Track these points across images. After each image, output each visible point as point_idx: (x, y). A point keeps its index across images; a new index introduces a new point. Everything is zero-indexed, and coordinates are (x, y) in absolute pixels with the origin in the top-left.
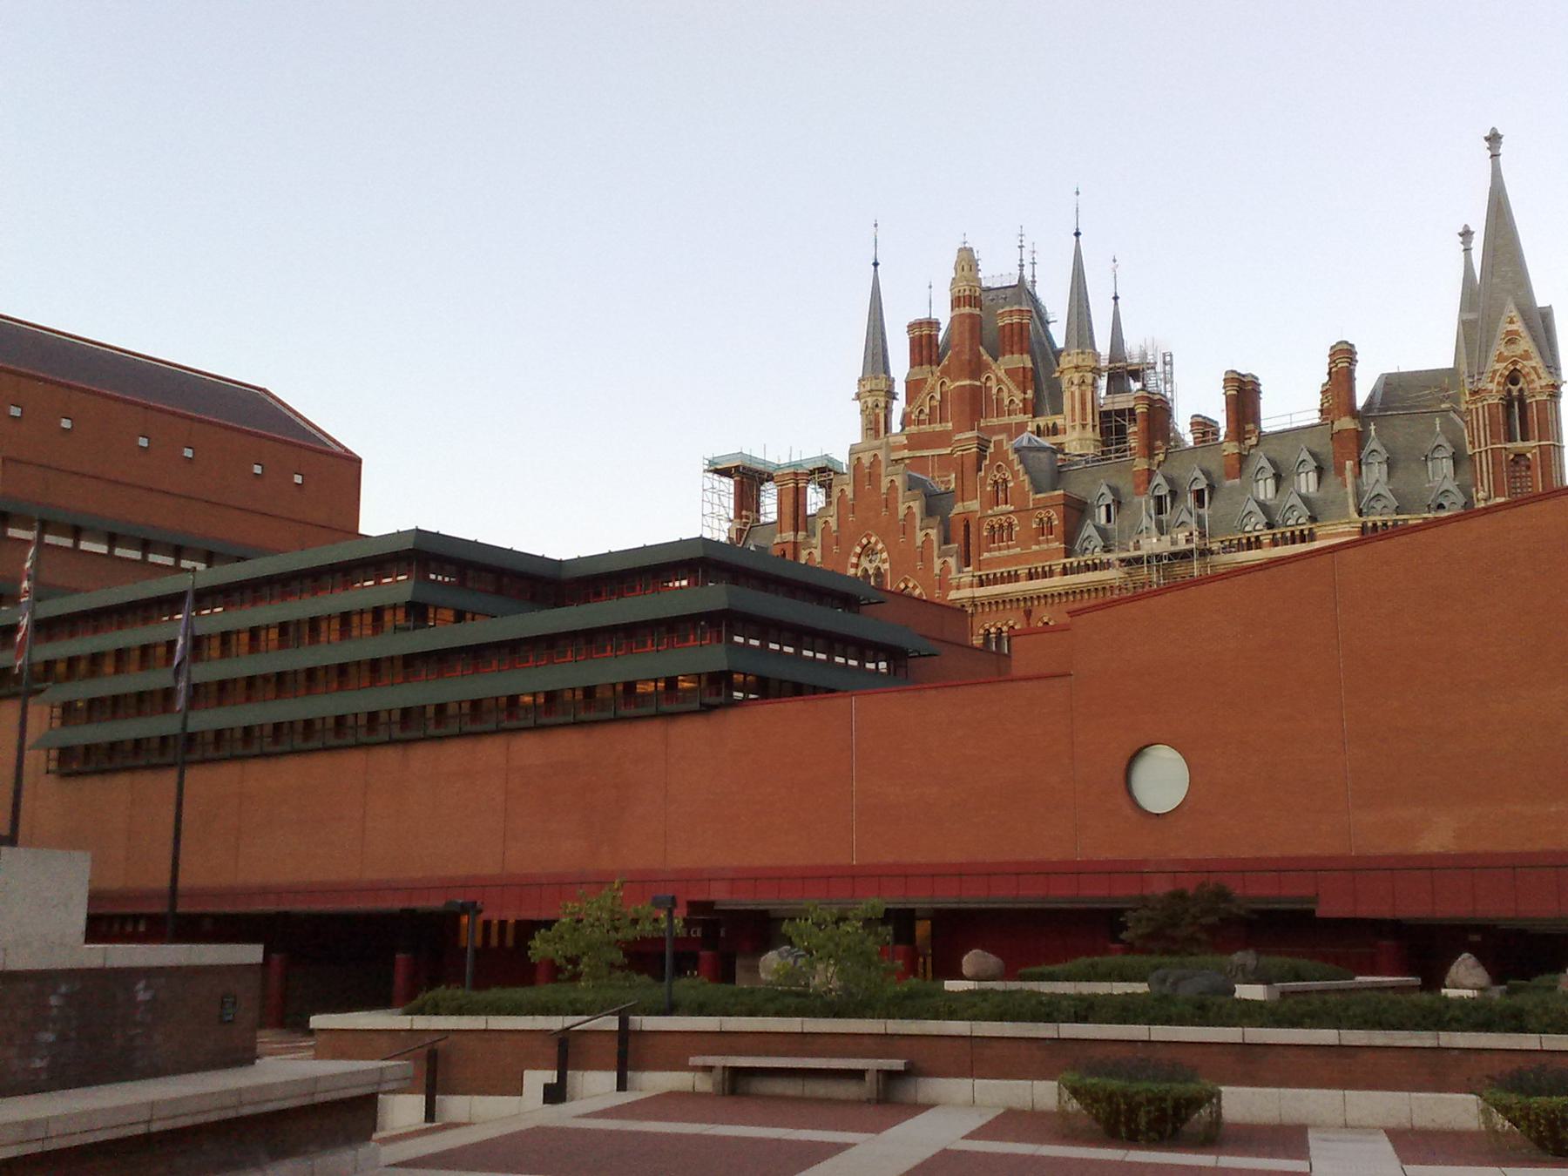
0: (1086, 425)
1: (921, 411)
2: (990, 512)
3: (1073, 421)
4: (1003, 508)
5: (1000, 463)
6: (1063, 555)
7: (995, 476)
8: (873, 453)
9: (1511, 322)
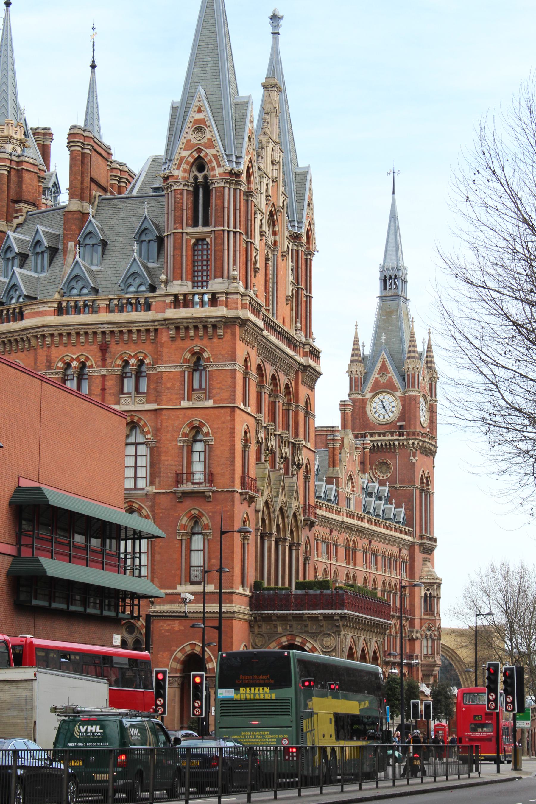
9: (200, 111)
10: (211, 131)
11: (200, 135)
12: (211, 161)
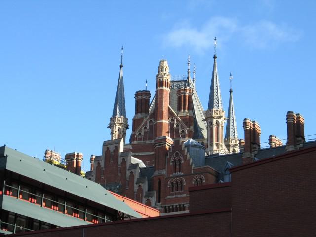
1: (140, 134)
7: (175, 158)
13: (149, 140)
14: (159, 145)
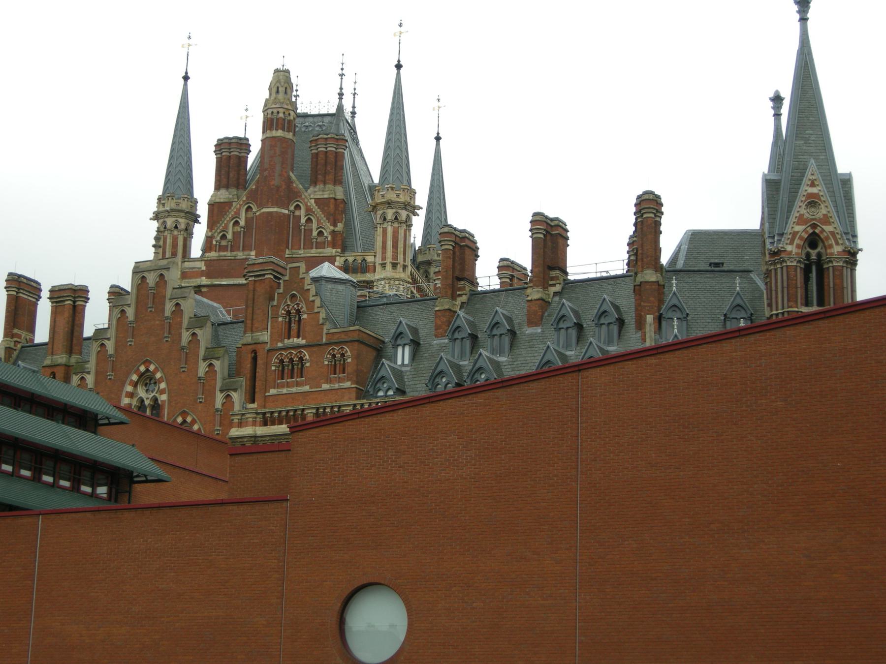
0: (397, 264)
1: (224, 237)
2: (280, 345)
3: (384, 258)
4: (296, 341)
5: (294, 292)
6: (354, 395)
8: (159, 272)
9: (813, 185)
10: (826, 207)
11: (813, 209)
12: (827, 238)
13: (243, 250)
14: (255, 276)
